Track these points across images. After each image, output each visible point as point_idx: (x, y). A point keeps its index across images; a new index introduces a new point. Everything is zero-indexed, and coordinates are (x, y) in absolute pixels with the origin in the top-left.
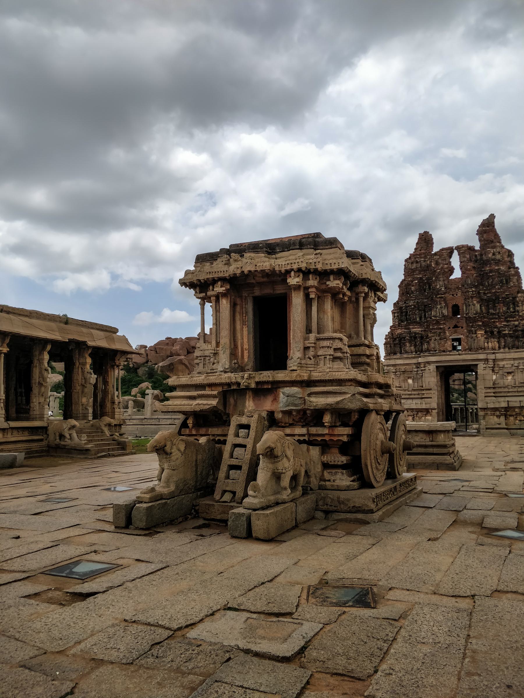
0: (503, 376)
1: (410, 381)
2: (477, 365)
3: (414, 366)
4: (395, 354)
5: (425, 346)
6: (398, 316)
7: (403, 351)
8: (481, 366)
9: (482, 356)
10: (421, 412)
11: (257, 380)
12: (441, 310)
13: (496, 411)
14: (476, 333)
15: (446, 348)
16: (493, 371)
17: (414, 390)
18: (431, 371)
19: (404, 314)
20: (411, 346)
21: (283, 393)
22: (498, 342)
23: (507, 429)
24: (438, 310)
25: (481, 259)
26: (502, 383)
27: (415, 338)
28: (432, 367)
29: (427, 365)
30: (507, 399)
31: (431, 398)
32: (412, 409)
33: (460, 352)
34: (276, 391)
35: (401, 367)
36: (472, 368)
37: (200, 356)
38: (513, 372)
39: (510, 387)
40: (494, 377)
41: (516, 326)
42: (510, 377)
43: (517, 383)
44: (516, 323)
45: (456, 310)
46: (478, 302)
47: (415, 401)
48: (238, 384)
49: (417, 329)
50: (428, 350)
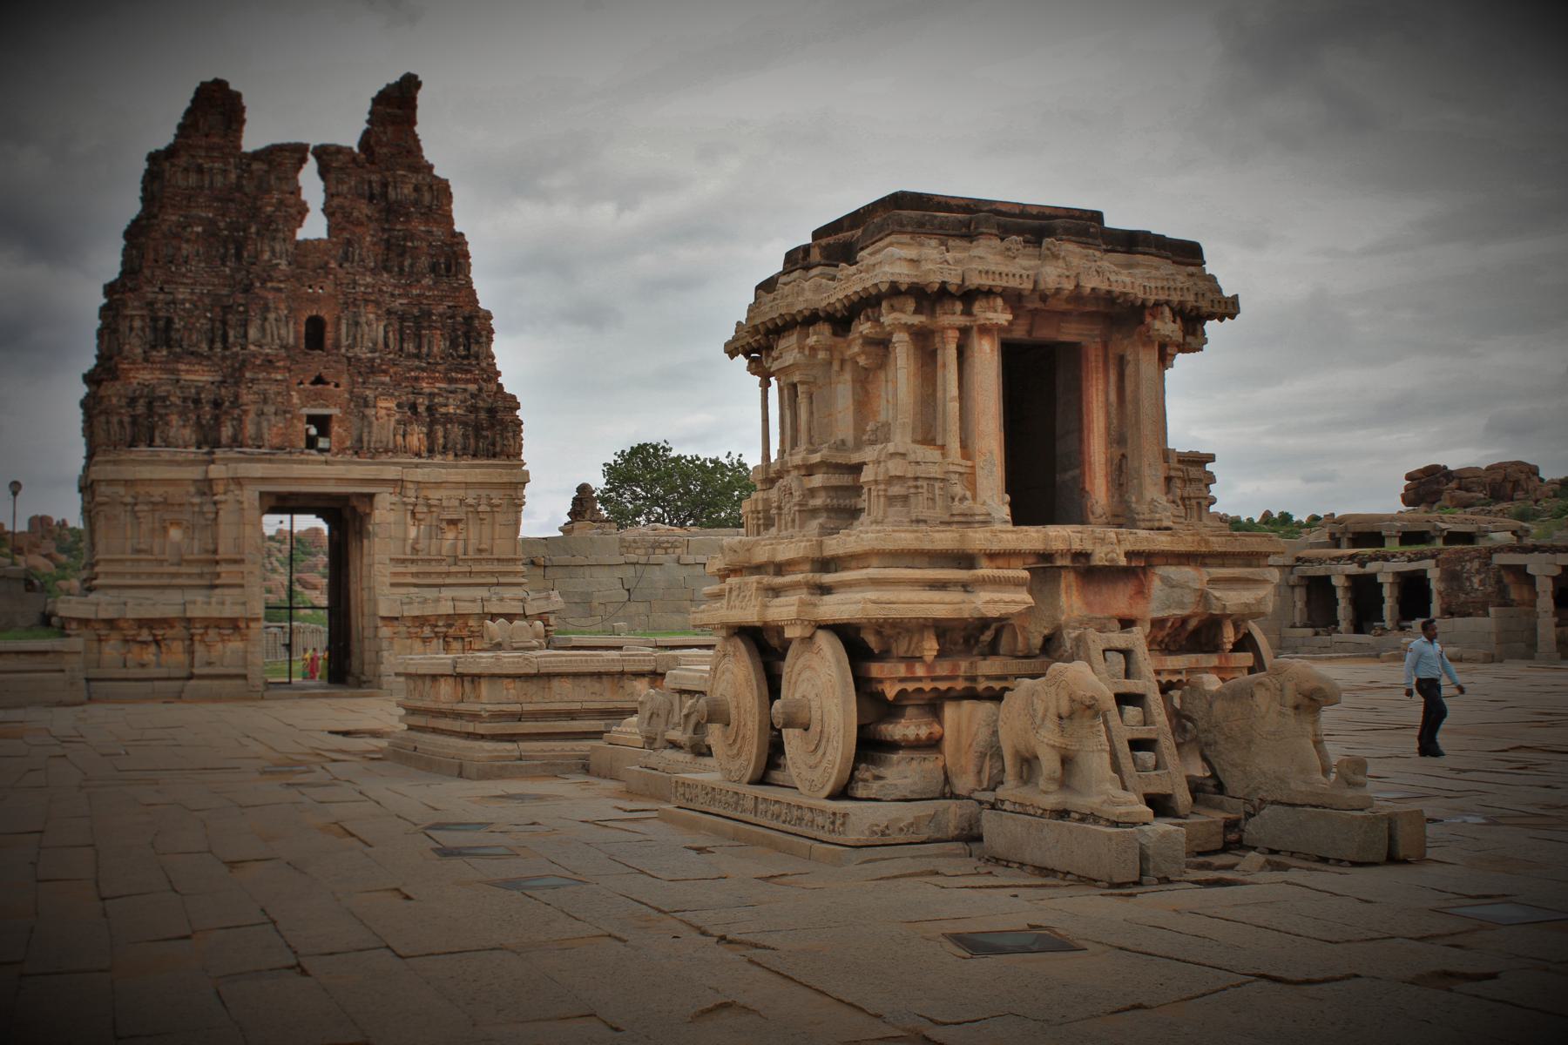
0: (436, 530)
1: (175, 534)
2: (371, 496)
3: (192, 489)
5: (227, 432)
6: (143, 329)
7: (158, 441)
9: (391, 473)
10: (217, 627)
11: (1129, 548)
12: (278, 330)
13: (422, 626)
16: (413, 513)
17: (190, 562)
18: (246, 505)
19: (161, 323)
21: (1166, 580)
22: (430, 435)
25: (385, 195)
26: (434, 551)
27: (197, 401)
28: (250, 495)
30: (447, 593)
31: (242, 586)
32: (189, 620)
33: (328, 456)
34: (1145, 574)
36: (354, 502)
37: (916, 479)
38: (460, 520)
39: (451, 560)
40: (413, 532)
41: (473, 396)
42: (450, 535)
44: (472, 387)
45: (315, 333)
46: (378, 318)
47: (189, 595)
48: (1085, 555)
49: (199, 376)
50: (236, 442)
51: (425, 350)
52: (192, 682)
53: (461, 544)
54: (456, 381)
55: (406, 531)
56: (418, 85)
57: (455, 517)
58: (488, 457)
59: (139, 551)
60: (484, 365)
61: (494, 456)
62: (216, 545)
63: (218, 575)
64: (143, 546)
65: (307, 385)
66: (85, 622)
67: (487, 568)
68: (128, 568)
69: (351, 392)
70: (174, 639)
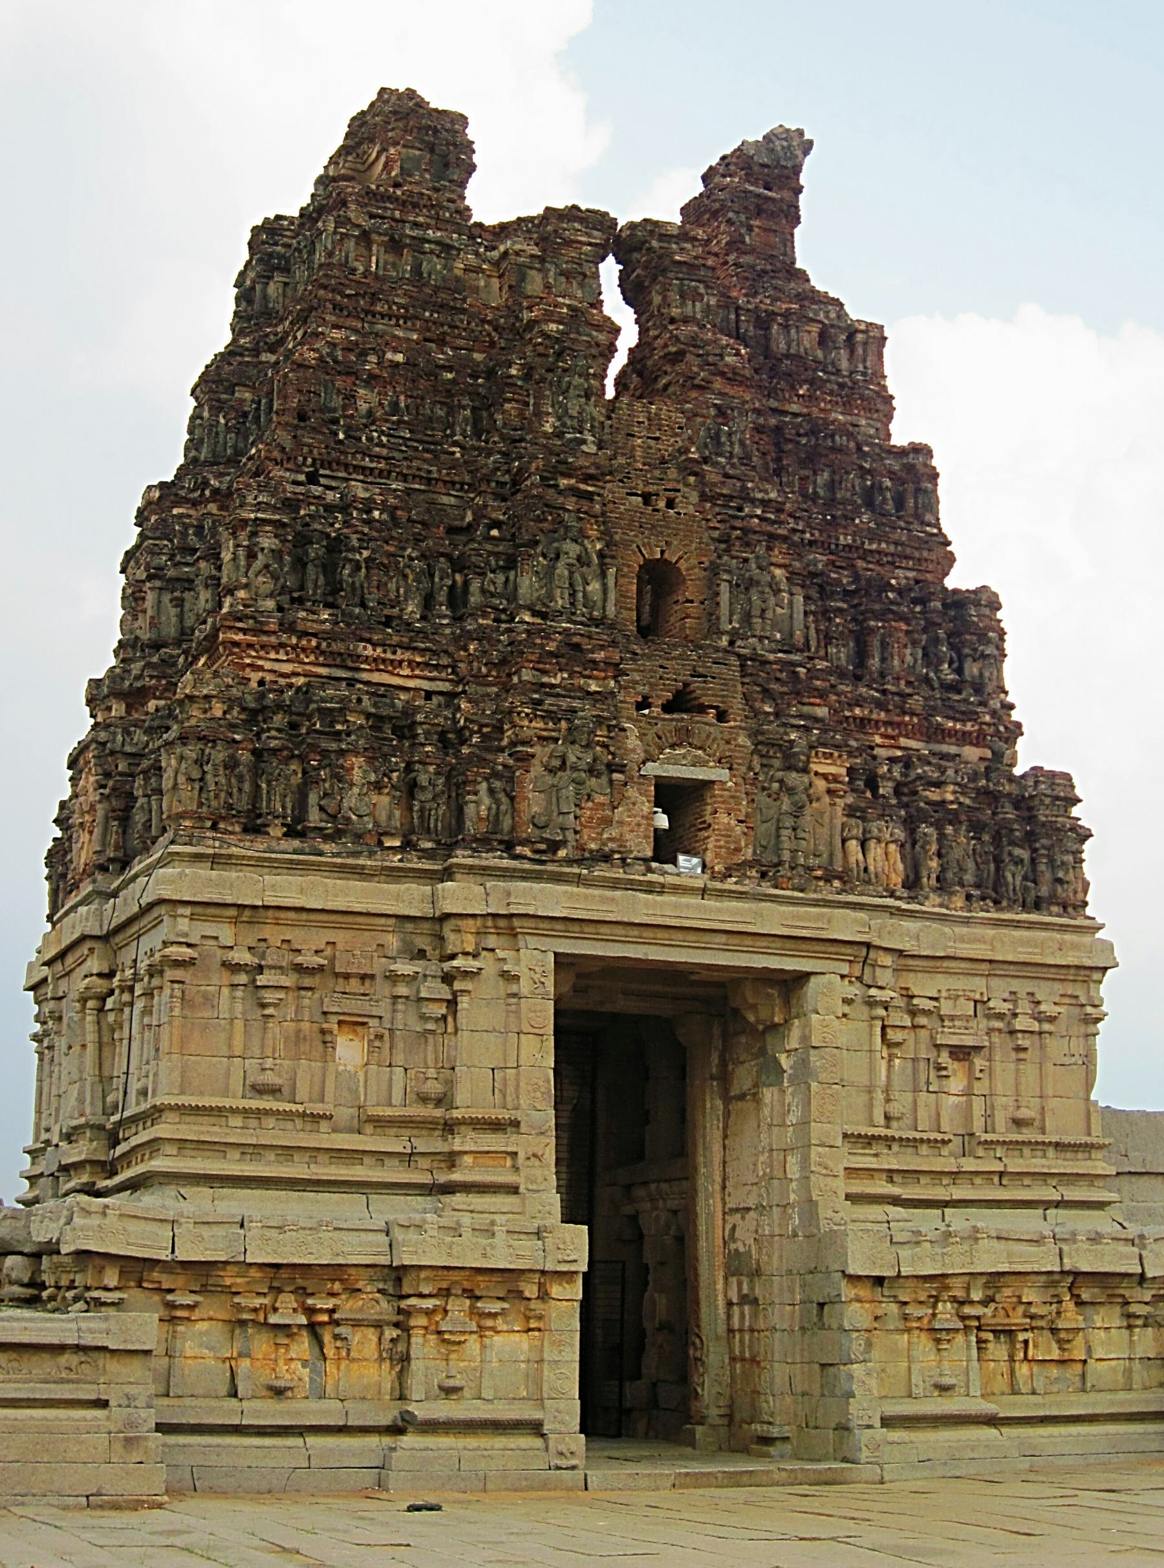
1: (349, 1051)
3: (393, 942)
4: (254, 828)
5: (479, 805)
6: (277, 554)
7: (314, 817)
8: (829, 988)
9: (846, 925)
14: (805, 770)
15: (620, 840)
17: (380, 1123)
18: (524, 987)
20: (378, 787)
23: (992, 1421)
24: (561, 570)
27: (405, 728)
28: (534, 962)
29: (491, 941)
31: (514, 1190)
35: (296, 936)
38: (978, 1049)
43: (1001, 1120)
51: (875, 663)
52: (408, 1440)
53: (978, 1105)
54: (941, 734)
55: (872, 1069)
56: (808, 146)
57: (969, 1041)
58: (1025, 907)
59: (260, 1090)
60: (995, 704)
61: (1037, 906)
62: (450, 1083)
63: (451, 1159)
64: (270, 1078)
65: (656, 710)
66: (136, 1269)
67: (1037, 1164)
68: (234, 1131)
69: (754, 734)
70: (357, 1324)
